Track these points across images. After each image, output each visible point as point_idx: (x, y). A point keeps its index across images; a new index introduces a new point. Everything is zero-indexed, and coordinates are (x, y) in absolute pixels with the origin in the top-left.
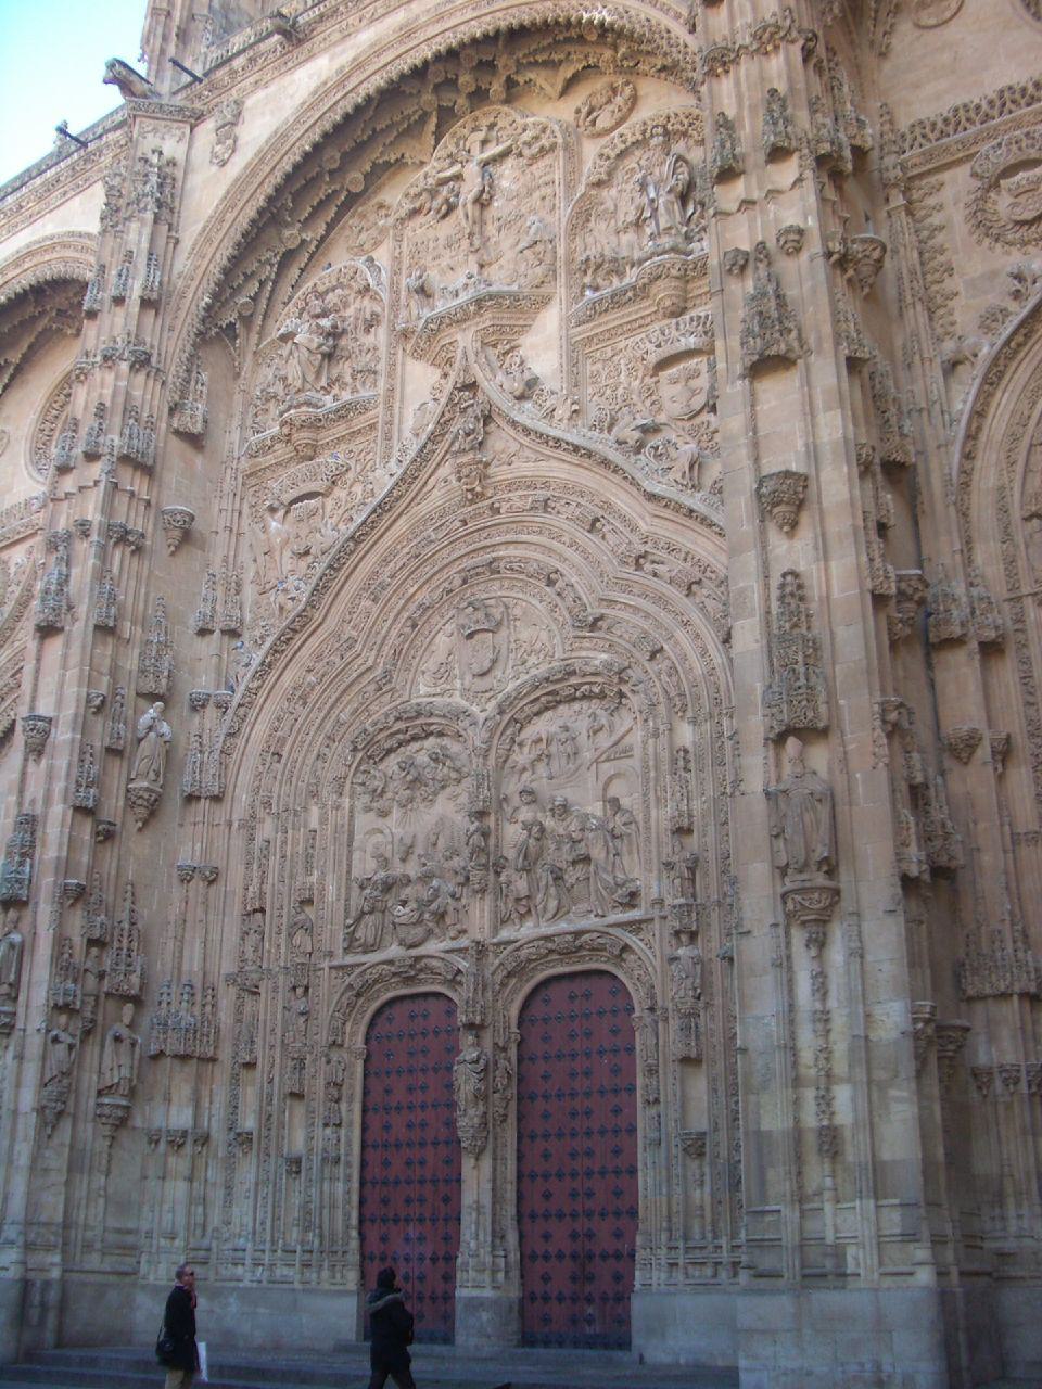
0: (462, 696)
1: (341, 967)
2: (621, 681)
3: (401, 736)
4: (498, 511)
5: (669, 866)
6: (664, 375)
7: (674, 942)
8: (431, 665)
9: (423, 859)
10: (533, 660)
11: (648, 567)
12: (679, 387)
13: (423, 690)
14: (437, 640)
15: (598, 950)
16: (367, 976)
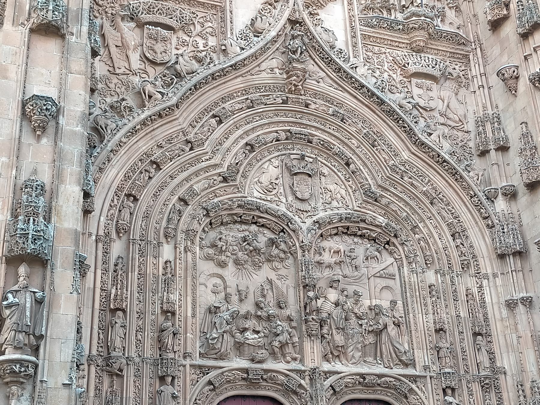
3: (235, 218)
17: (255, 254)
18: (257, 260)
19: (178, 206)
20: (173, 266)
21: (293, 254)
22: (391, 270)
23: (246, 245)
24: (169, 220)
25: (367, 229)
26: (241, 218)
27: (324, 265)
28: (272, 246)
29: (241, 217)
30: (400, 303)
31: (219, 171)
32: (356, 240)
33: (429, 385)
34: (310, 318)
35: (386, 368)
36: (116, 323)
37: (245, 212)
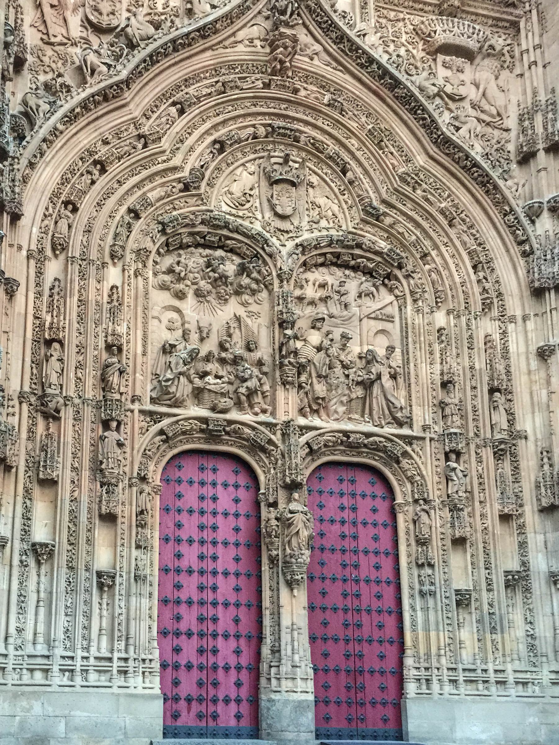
0: (264, 228)
1: (151, 413)
2: (400, 267)
4: (296, 91)
5: (442, 405)
6: (440, 58)
7: (442, 457)
8: (236, 189)
9: (227, 345)
10: (324, 223)
11: (419, 192)
12: (448, 73)
13: (225, 208)
14: (238, 171)
15: (379, 451)
16: (178, 428)
17: (220, 283)
18: (223, 291)
19: (127, 219)
20: (120, 292)
21: (268, 287)
22: (388, 310)
23: (210, 271)
24: (116, 235)
25: (362, 257)
26: (205, 240)
27: (306, 301)
28: (243, 275)
29: (204, 237)
30: (398, 351)
31: (177, 176)
32: (347, 272)
33: (428, 448)
34: (286, 361)
35: (376, 426)
36: (51, 355)
37: (210, 230)
